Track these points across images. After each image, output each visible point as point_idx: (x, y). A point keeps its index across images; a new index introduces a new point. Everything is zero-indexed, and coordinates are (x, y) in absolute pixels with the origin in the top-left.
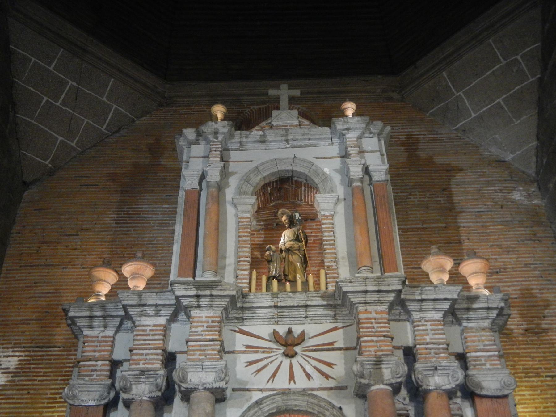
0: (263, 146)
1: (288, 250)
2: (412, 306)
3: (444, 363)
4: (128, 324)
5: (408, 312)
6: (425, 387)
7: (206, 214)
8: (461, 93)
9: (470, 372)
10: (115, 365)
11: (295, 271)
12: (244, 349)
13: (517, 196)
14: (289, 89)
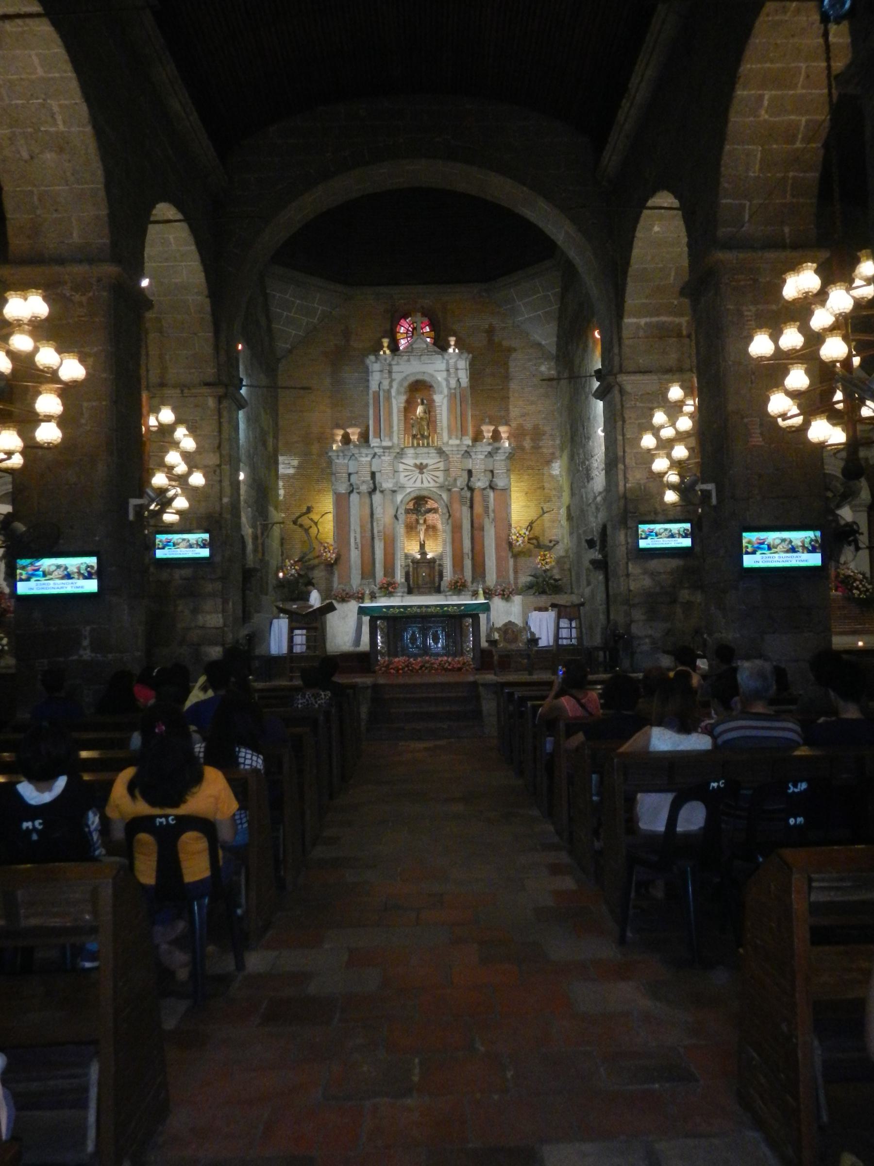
0: (409, 363)
1: (421, 418)
2: (472, 454)
3: (482, 478)
4: (353, 458)
5: (471, 456)
6: (474, 487)
10: (350, 474)
11: (424, 429)
12: (402, 470)
13: (543, 368)
14: (422, 317)
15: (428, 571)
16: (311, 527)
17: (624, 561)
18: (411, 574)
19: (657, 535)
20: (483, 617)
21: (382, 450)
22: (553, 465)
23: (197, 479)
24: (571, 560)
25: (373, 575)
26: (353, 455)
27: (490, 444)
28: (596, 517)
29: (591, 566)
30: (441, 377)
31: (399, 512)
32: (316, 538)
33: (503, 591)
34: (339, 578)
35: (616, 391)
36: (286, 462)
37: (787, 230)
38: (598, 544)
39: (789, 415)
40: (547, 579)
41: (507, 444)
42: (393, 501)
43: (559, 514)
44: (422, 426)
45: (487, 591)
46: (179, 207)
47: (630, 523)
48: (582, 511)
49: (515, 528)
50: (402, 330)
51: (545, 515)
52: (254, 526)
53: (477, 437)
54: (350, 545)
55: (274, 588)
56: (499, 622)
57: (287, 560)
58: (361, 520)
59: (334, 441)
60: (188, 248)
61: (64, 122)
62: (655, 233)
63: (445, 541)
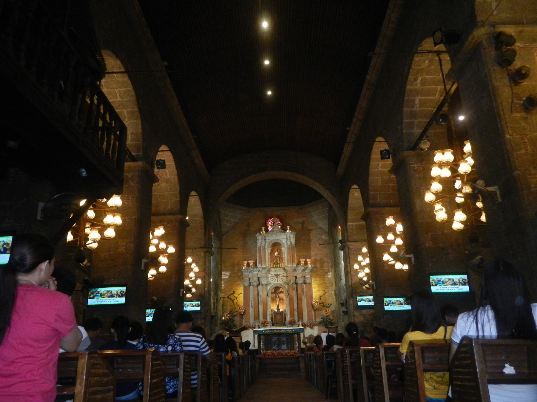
1: (277, 256)
2: (297, 270)
3: (301, 279)
4: (251, 272)
5: (296, 271)
6: (298, 283)
7: (263, 253)
8: (314, 213)
9: (305, 280)
10: (249, 278)
13: (323, 237)
15: (280, 316)
16: (234, 299)
17: (353, 311)
18: (274, 318)
19: (364, 300)
20: (302, 335)
21: (262, 269)
22: (329, 274)
23: (199, 282)
24: (337, 311)
25: (258, 319)
26: (251, 271)
27: (303, 266)
28: (344, 294)
29: (343, 314)
30: (284, 241)
31: (269, 293)
32: (236, 304)
33: (310, 324)
34: (245, 320)
35: (346, 248)
36: (225, 274)
37: (391, 201)
38: (345, 304)
39: (390, 261)
40: (328, 320)
41: (310, 266)
42: (266, 289)
43: (331, 293)
44: (278, 259)
45: (304, 325)
46: (197, 192)
47: (354, 296)
48: (339, 292)
49: (314, 299)
50: (269, 223)
51: (327, 294)
52: (214, 299)
53: (299, 264)
54: (249, 306)
55: (220, 324)
56: (307, 335)
57: (225, 313)
58: (254, 296)
59: (244, 266)
60: (198, 203)
61: (169, 175)
62: (356, 195)
63: (287, 305)
